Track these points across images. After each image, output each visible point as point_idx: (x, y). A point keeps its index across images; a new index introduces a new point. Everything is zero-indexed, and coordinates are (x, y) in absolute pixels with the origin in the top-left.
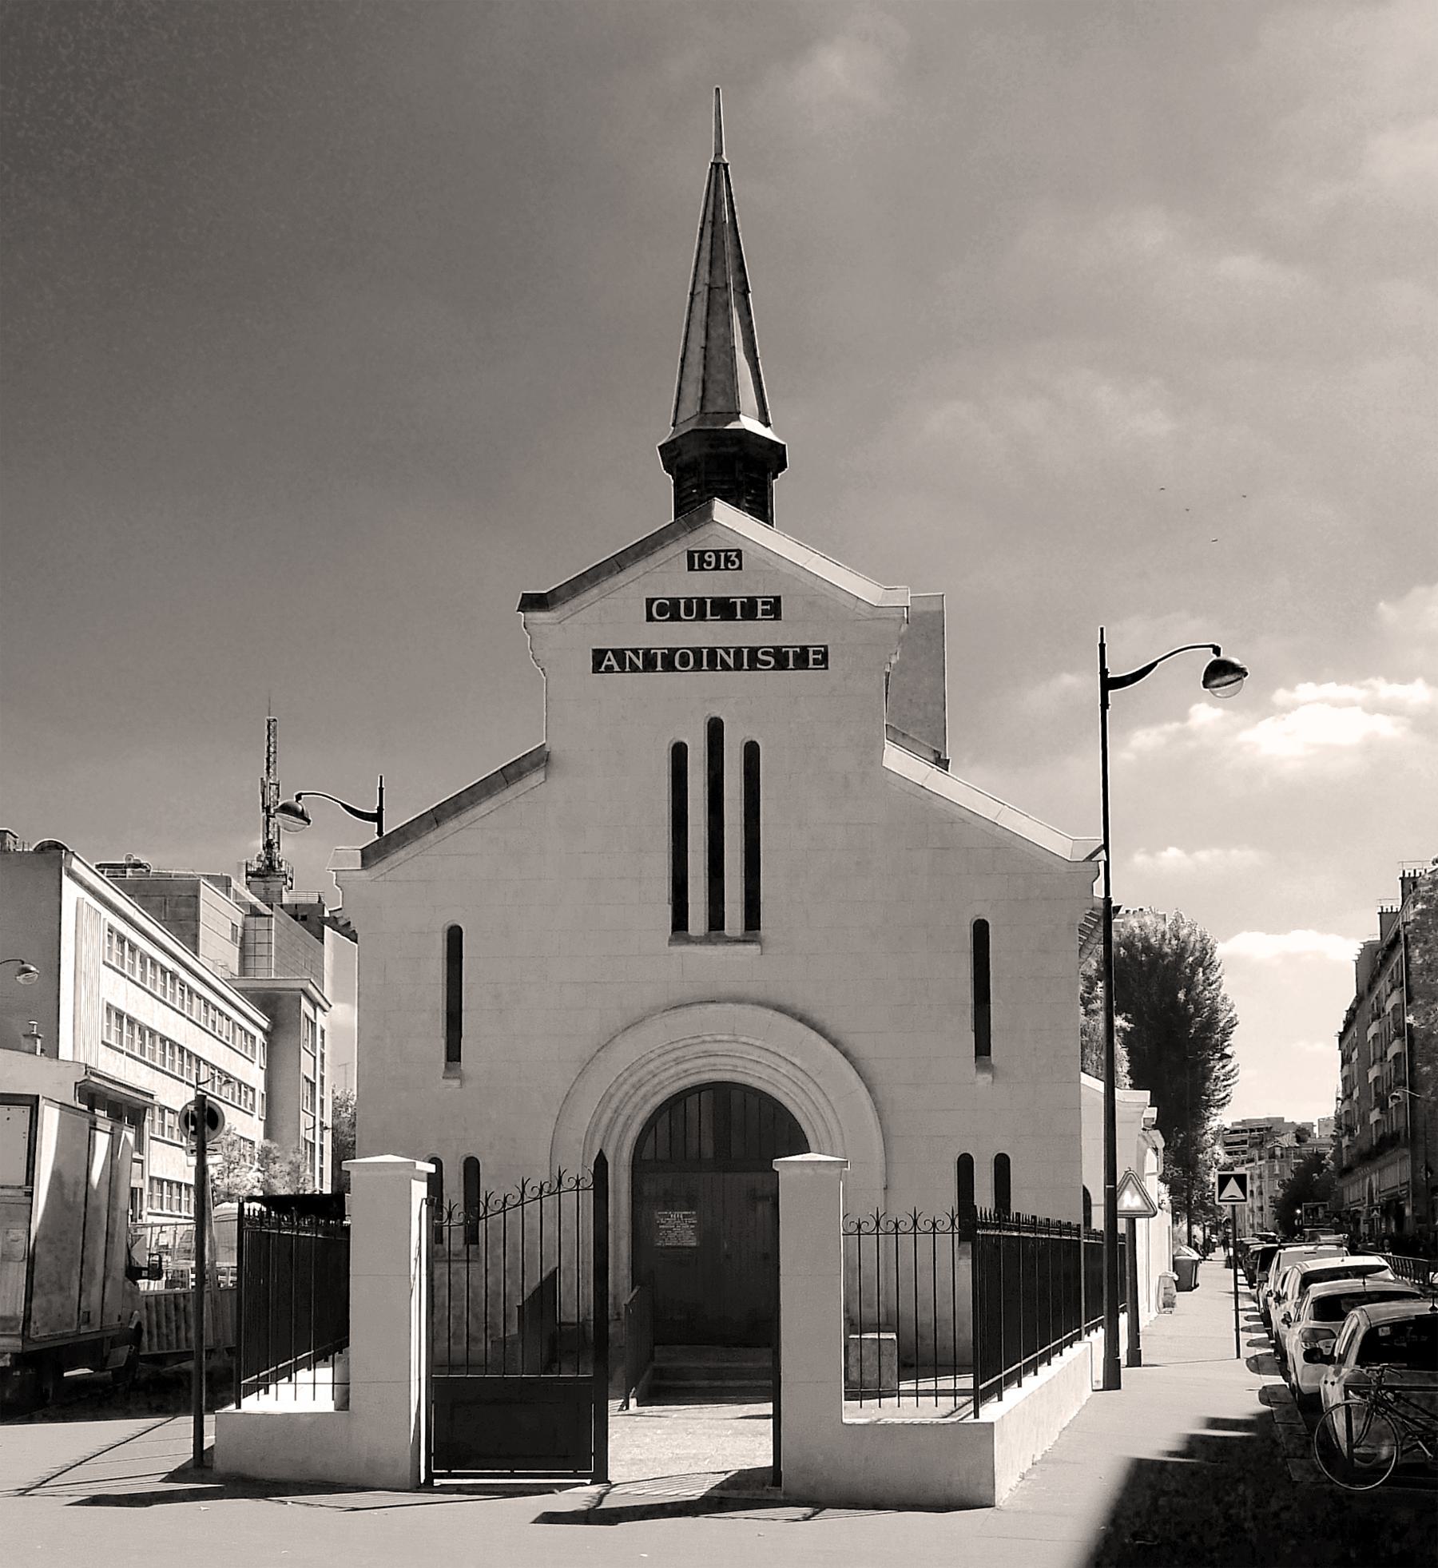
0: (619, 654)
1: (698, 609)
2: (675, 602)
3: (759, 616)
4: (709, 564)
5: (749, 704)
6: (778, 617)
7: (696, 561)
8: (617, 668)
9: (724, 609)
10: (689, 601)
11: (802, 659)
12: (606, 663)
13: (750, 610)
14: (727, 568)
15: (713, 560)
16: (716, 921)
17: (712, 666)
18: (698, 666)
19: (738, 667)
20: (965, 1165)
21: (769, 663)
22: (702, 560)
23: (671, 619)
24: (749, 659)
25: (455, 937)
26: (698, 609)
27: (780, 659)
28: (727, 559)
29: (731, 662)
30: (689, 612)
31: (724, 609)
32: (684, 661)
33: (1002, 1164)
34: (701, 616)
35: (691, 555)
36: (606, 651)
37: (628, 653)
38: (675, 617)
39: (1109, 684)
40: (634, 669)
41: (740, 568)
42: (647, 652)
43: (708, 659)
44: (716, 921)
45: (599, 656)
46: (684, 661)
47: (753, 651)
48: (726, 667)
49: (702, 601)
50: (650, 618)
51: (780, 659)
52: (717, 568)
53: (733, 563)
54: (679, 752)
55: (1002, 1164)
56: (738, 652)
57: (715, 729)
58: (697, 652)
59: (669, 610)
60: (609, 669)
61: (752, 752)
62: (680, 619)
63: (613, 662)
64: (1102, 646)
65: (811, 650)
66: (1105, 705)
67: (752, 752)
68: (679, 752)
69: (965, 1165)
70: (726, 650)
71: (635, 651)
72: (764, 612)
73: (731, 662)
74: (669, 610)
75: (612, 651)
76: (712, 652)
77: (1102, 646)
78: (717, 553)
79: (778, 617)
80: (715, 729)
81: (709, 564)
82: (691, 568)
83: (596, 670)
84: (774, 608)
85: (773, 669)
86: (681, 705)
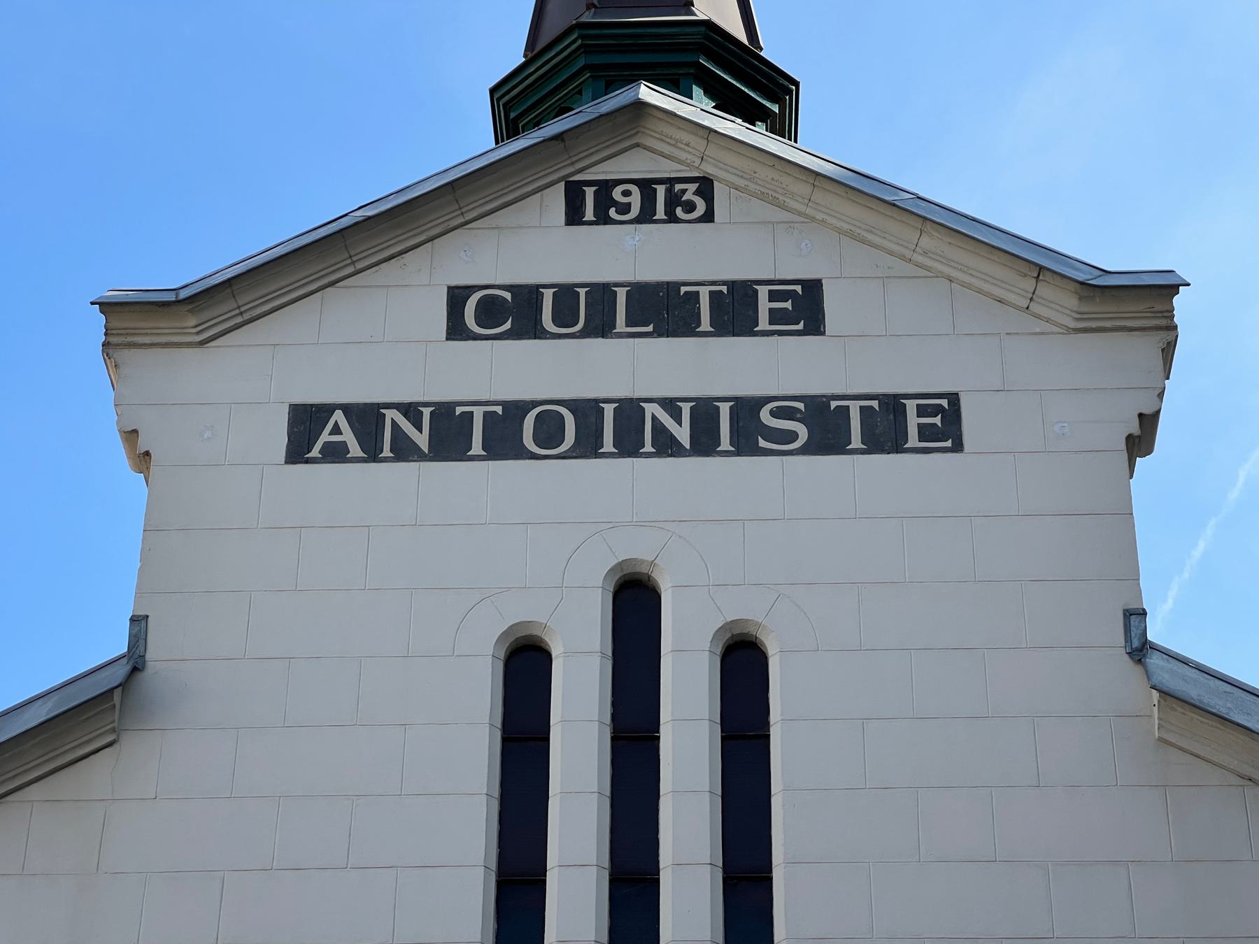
0: (366, 418)
1: (591, 311)
2: (528, 296)
3: (764, 324)
4: (625, 209)
5: (730, 541)
7: (589, 204)
8: (355, 449)
9: (664, 309)
10: (566, 293)
11: (886, 425)
12: (325, 437)
13: (735, 310)
14: (672, 218)
15: (636, 200)
17: (628, 446)
18: (588, 446)
19: (704, 443)
21: (791, 436)
23: (514, 335)
24: (731, 427)
26: (591, 311)
27: (824, 427)
28: (673, 200)
29: (683, 434)
30: (564, 315)
31: (664, 309)
32: (549, 432)
35: (574, 195)
36: (328, 409)
37: (390, 414)
38: (529, 328)
40: (404, 451)
41: (708, 217)
47: (746, 409)
48: (666, 446)
50: (456, 330)
51: (824, 427)
52: (646, 216)
53: (690, 207)
54: (526, 665)
56: (704, 412)
57: (635, 605)
58: (587, 410)
60: (335, 454)
61: (743, 663)
62: (537, 332)
63: (348, 436)
65: (911, 405)
67: (743, 663)
68: (526, 665)
70: (670, 405)
71: (411, 411)
72: (775, 316)
73: (683, 434)
75: (347, 409)
78: (646, 186)
80: (635, 605)
81: (625, 209)
82: (574, 216)
83: (297, 453)
84: (805, 308)
85: (805, 450)
86: (535, 544)
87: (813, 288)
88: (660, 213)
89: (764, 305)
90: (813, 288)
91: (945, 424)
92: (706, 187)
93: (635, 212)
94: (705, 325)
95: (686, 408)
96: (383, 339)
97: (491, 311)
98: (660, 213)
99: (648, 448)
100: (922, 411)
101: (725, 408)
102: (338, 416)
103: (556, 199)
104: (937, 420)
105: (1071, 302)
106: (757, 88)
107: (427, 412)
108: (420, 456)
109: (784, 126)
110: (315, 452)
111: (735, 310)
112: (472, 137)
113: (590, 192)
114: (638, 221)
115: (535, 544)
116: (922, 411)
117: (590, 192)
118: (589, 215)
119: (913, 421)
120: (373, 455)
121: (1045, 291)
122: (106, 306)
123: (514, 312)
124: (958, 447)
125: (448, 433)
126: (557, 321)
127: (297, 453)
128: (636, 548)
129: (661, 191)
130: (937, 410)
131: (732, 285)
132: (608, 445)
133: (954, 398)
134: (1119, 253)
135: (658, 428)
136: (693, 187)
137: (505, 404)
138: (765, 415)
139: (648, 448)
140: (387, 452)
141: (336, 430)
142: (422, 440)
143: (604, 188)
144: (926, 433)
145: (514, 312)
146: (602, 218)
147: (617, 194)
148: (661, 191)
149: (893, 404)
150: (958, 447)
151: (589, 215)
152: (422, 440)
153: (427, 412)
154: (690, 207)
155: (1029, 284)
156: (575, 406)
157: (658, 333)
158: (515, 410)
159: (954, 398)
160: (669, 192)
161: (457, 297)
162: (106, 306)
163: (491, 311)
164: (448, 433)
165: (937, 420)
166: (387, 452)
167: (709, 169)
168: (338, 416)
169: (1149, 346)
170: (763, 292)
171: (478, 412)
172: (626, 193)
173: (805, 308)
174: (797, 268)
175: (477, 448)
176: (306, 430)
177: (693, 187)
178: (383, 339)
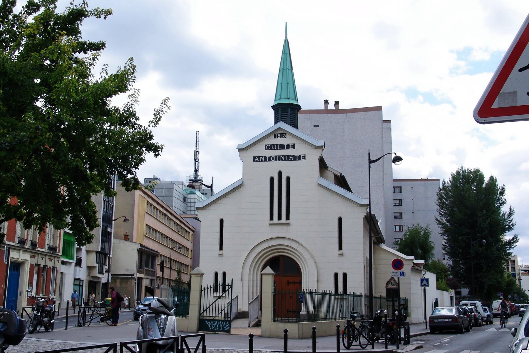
0: (259, 157)
1: (276, 147)
2: (271, 145)
5: (288, 168)
6: (294, 148)
9: (282, 147)
10: (274, 145)
13: (288, 147)
16: (280, 218)
17: (279, 160)
18: (276, 160)
19: (285, 160)
20: (336, 275)
22: (277, 136)
24: (287, 158)
26: (276, 147)
27: (295, 158)
28: (283, 135)
29: (284, 159)
31: (282, 147)
32: (273, 159)
33: (345, 275)
34: (277, 149)
35: (275, 135)
38: (271, 149)
39: (371, 162)
40: (262, 161)
42: (265, 157)
43: (278, 158)
44: (280, 218)
46: (273, 159)
47: (289, 156)
48: (282, 160)
49: (277, 145)
50: (266, 149)
51: (295, 158)
54: (272, 179)
55: (345, 275)
56: (285, 156)
57: (280, 173)
58: (276, 156)
59: (270, 147)
60: (257, 161)
61: (288, 179)
64: (369, 153)
66: (370, 167)
67: (288, 179)
68: (272, 179)
69: (336, 275)
70: (283, 156)
71: (262, 157)
73: (284, 159)
74: (270, 147)
76: (279, 156)
77: (369, 153)
78: (281, 134)
79: (294, 148)
80: (280, 173)
82: (275, 138)
83: (254, 161)
84: (293, 146)
87: (294, 144)
91: (304, 158)
97: (268, 147)
111: (288, 147)
125: (265, 159)
127: (254, 161)
145: (270, 147)
149: (300, 156)
158: (271, 157)
161: (266, 146)
164: (265, 159)
173: (293, 146)
176: (254, 158)
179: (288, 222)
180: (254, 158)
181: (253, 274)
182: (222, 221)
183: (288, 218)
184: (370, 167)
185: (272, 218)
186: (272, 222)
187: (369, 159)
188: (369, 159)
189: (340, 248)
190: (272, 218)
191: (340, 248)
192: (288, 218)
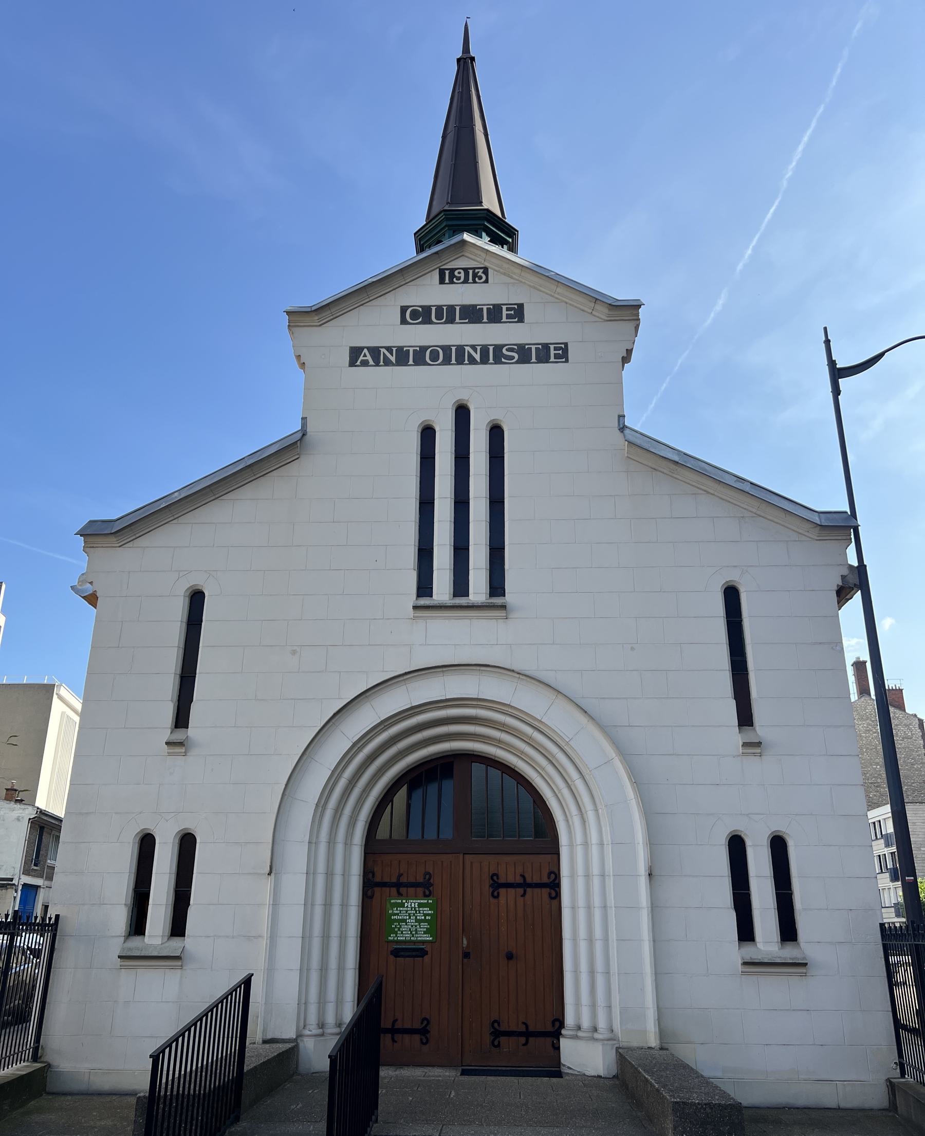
0: (375, 352)
1: (447, 314)
2: (427, 310)
3: (504, 319)
4: (459, 278)
5: (493, 392)
6: (521, 320)
7: (447, 277)
8: (371, 362)
9: (471, 314)
10: (439, 309)
11: (544, 354)
12: (361, 358)
13: (494, 314)
14: (474, 282)
15: (462, 275)
16: (461, 586)
17: (460, 362)
18: (447, 361)
19: (484, 360)
21: (513, 358)
24: (493, 355)
25: (196, 599)
26: (447, 314)
27: (523, 354)
28: (475, 275)
29: (477, 357)
30: (439, 316)
31: (471, 314)
36: (362, 349)
37: (383, 350)
38: (427, 321)
39: (837, 373)
40: (387, 363)
41: (486, 281)
43: (455, 355)
44: (461, 586)
45: (355, 353)
47: (498, 348)
48: (472, 361)
49: (451, 308)
50: (404, 321)
51: (523, 354)
52: (466, 281)
54: (428, 434)
56: (485, 350)
57: (462, 414)
58: (446, 349)
60: (365, 364)
61: (496, 433)
62: (431, 322)
63: (369, 358)
64: (827, 342)
65: (552, 347)
66: (836, 391)
67: (496, 433)
68: (428, 434)
70: (474, 347)
71: (389, 349)
72: (508, 316)
73: (477, 357)
75: (368, 348)
77: (827, 342)
78: (466, 270)
79: (521, 320)
80: (462, 414)
81: (459, 278)
82: (442, 281)
83: (352, 364)
84: (518, 313)
85: (517, 362)
86: (430, 394)
87: (521, 306)
88: (471, 280)
89: (505, 313)
90: (521, 306)
91: (563, 353)
92: (486, 271)
93: (462, 279)
94: (485, 320)
95: (479, 348)
96: (380, 325)
97: (415, 315)
98: (471, 280)
99: (466, 362)
100: (555, 349)
101: (491, 348)
102: (365, 351)
103: (436, 275)
104: (560, 352)
105: (606, 311)
106: (503, 234)
107: (394, 349)
108: (393, 365)
109: (513, 248)
110: (358, 363)
111: (494, 314)
112: (408, 252)
113: (447, 272)
114: (463, 283)
115: (430, 394)
116: (555, 349)
117: (447, 272)
118: (447, 281)
119: (552, 352)
120: (377, 364)
121: (598, 307)
122: (288, 313)
123: (423, 315)
124: (567, 361)
125: (402, 357)
126: (437, 318)
127: (352, 364)
128: (463, 396)
129: (471, 272)
130: (560, 348)
131: (494, 305)
132: (453, 361)
133: (566, 344)
134: (622, 294)
135: (470, 355)
136: (481, 271)
137: (420, 347)
138: (504, 351)
139: (466, 362)
140: (382, 363)
141: (365, 356)
142: (393, 359)
143: (452, 271)
144: (556, 356)
145: (423, 315)
146: (451, 282)
147: (456, 273)
148: (471, 272)
149: (546, 346)
150: (567, 361)
151: (447, 281)
152: (393, 359)
153: (394, 349)
154: (480, 278)
155: (592, 305)
156: (442, 347)
157: (470, 322)
158: (423, 349)
159: (566, 344)
160: (474, 272)
161: (404, 310)
162: (288, 313)
163: (415, 315)
164: (402, 357)
165: (560, 352)
166: (382, 363)
167: (487, 264)
168: (365, 351)
169: (630, 326)
170: (504, 308)
171: (411, 350)
172: (459, 273)
173: (518, 313)
174: (515, 300)
175: (411, 362)
177: (481, 271)
178: (380, 325)
179: (498, 601)
180: (355, 353)
181: (331, 842)
182: (196, 599)
183: (497, 586)
184: (836, 391)
185: (424, 587)
186: (424, 601)
187: (832, 363)
188: (832, 363)
189: (745, 718)
190: (424, 587)
191: (745, 718)
192: (497, 586)
